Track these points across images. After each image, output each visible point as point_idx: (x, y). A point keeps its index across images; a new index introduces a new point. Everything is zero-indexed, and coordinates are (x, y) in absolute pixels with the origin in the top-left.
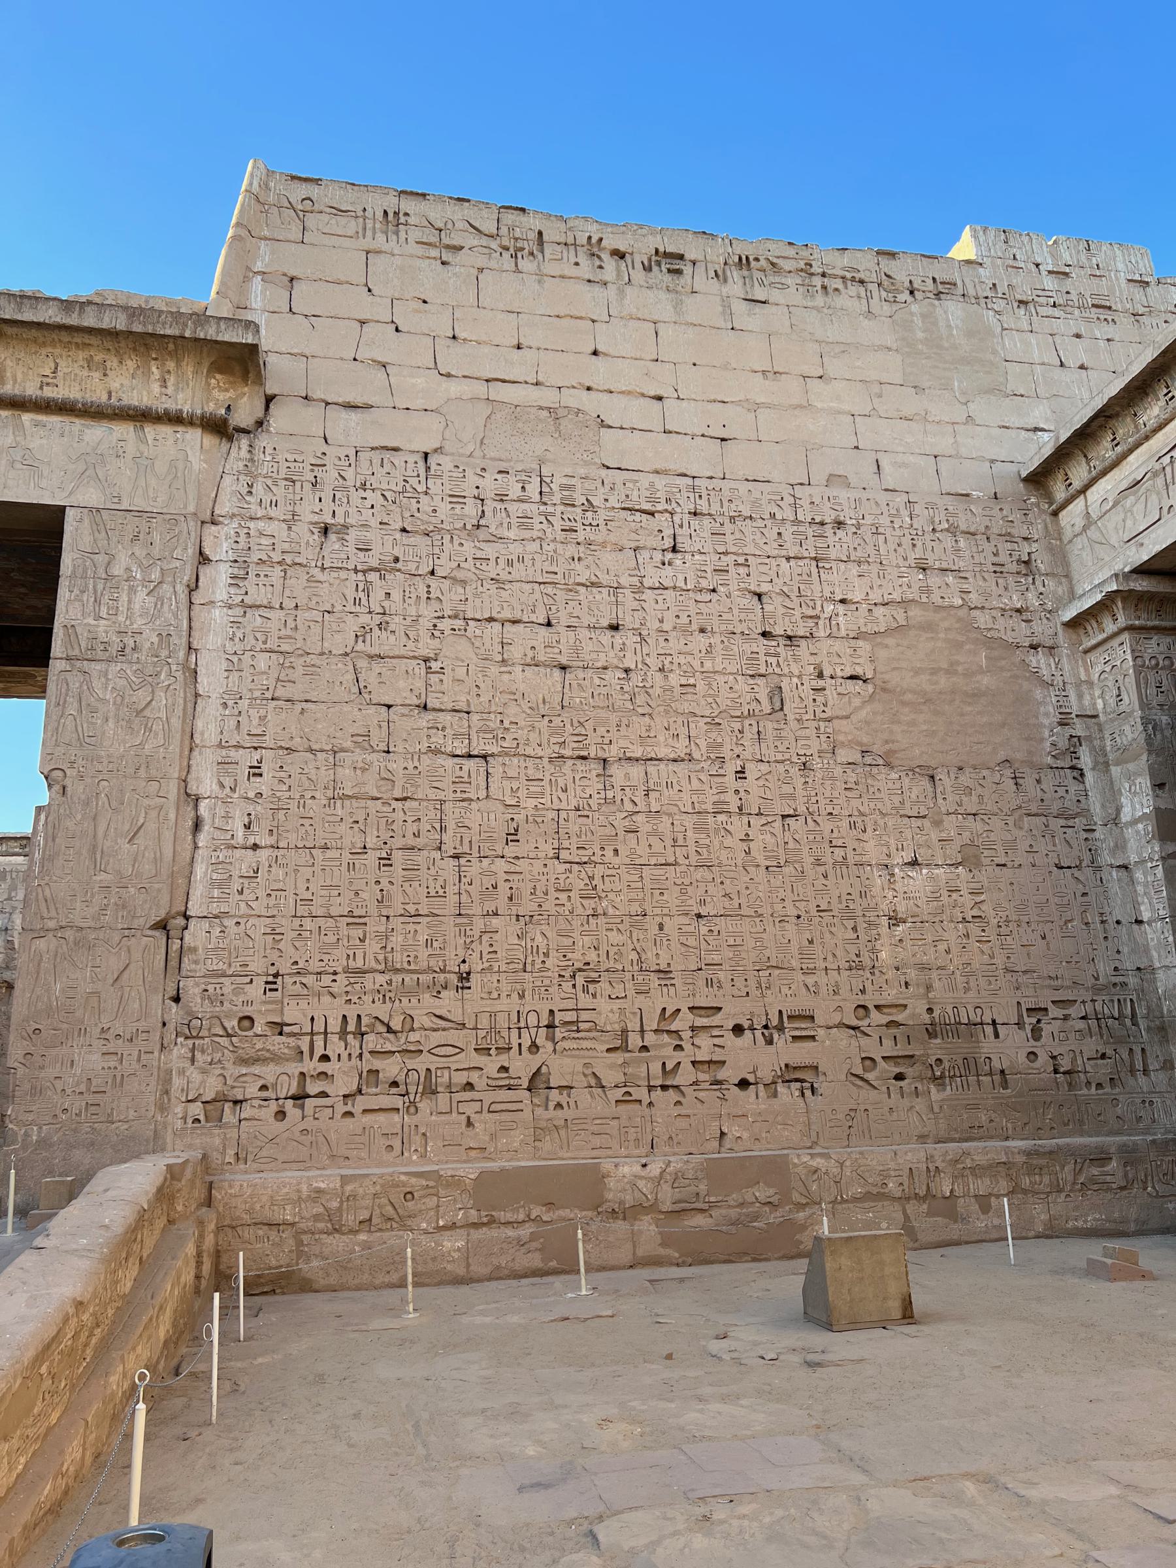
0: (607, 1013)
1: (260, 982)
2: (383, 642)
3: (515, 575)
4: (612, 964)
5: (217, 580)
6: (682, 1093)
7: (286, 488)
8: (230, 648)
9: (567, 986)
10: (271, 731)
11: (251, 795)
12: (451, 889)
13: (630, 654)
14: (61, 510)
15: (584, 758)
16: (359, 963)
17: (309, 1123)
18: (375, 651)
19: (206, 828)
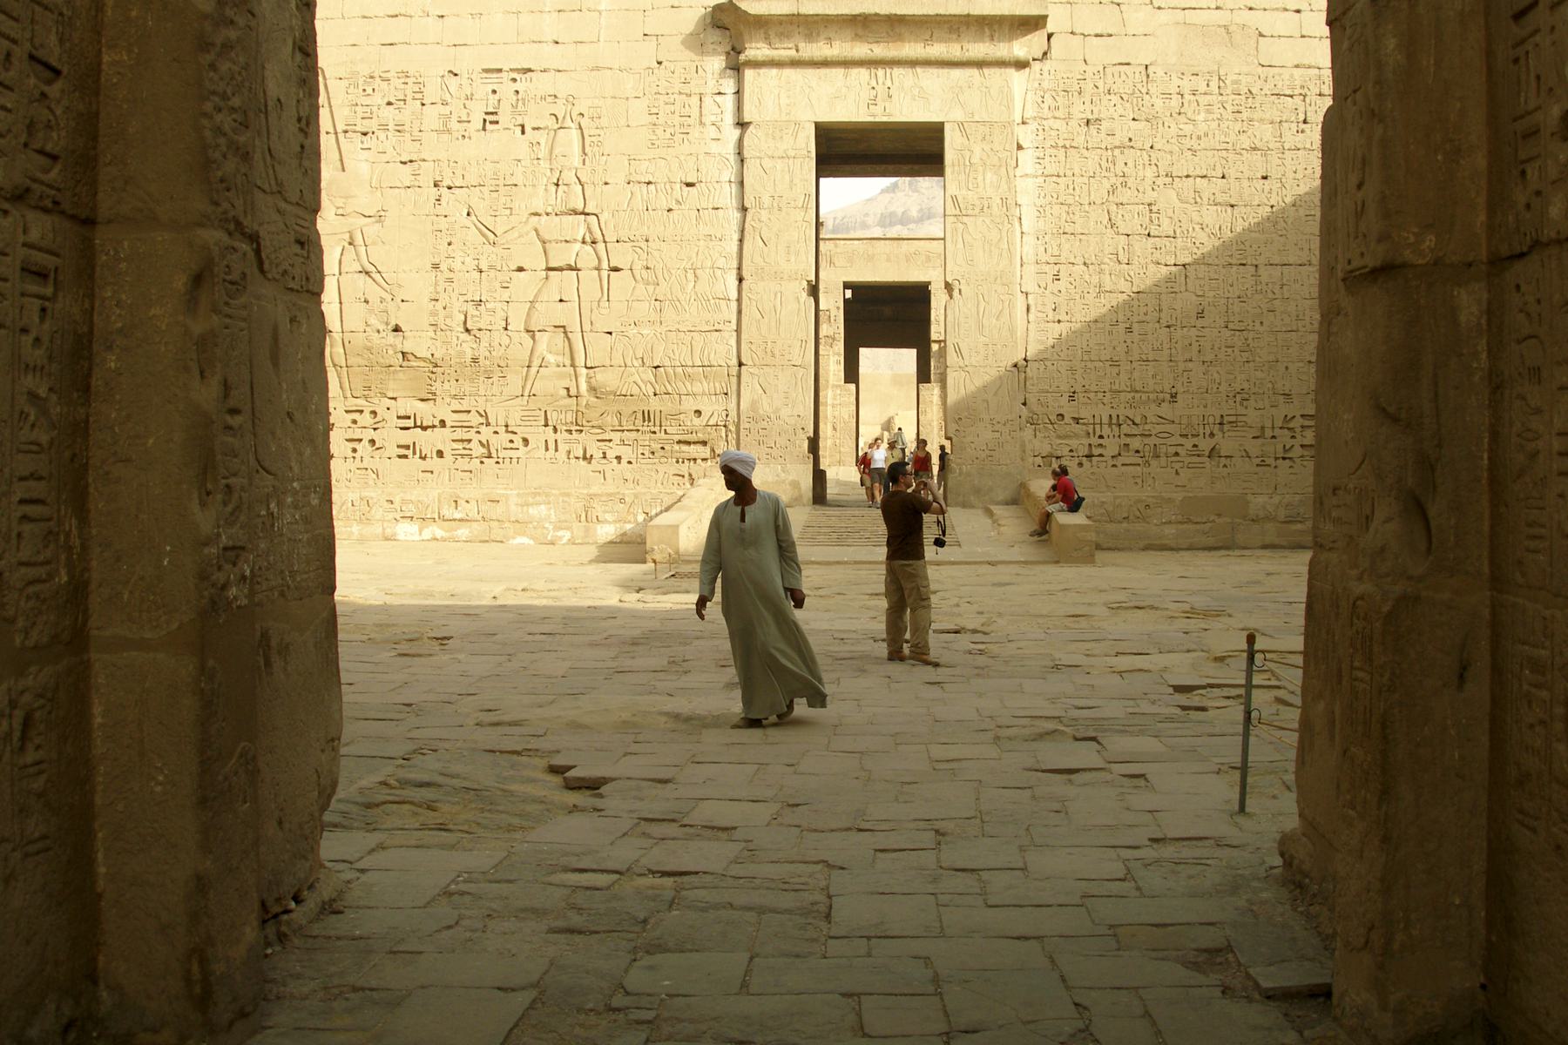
0: (1252, 417)
1: (1066, 396)
2: (1125, 195)
3: (1203, 146)
4: (1256, 390)
5: (1027, 159)
6: (1294, 462)
7: (1064, 97)
8: (1038, 203)
9: (1231, 402)
10: (1064, 255)
11: (1056, 292)
12: (1166, 346)
13: (1274, 194)
14: (943, 123)
15: (1244, 265)
16: (1116, 387)
17: (1095, 470)
18: (1118, 201)
19: (1033, 309)
